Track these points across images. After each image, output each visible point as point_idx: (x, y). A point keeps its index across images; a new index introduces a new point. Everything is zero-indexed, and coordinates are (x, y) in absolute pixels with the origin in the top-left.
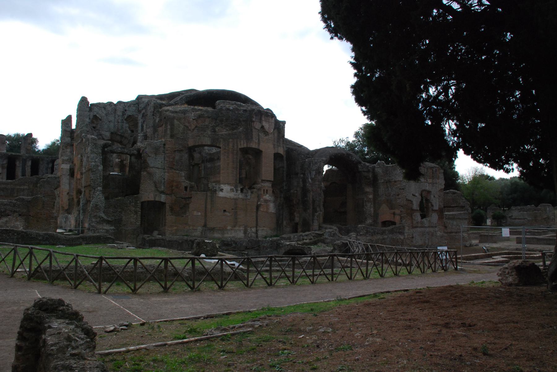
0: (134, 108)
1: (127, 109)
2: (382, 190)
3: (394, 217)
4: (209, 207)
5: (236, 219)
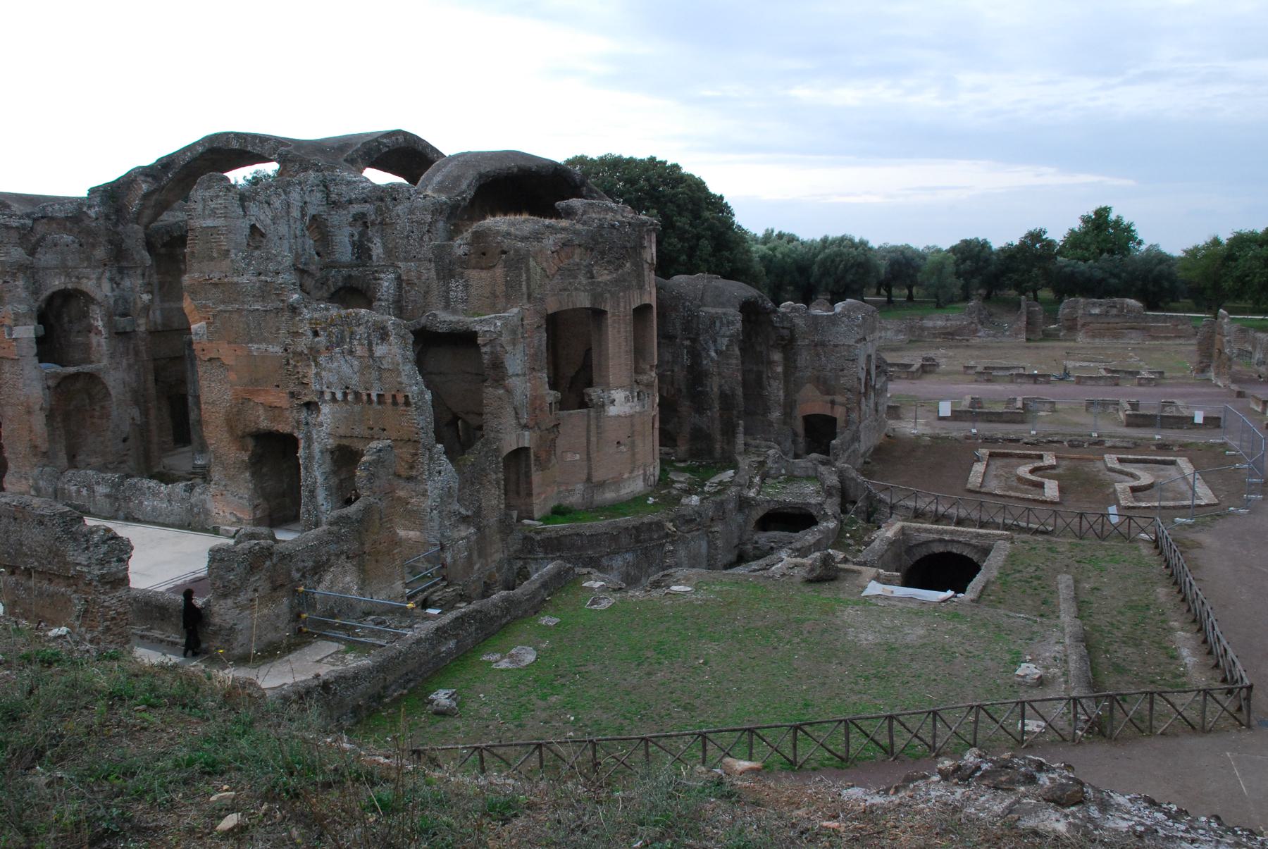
1: (308, 199)
2: (804, 358)
3: (832, 408)
4: (593, 439)
5: (634, 455)
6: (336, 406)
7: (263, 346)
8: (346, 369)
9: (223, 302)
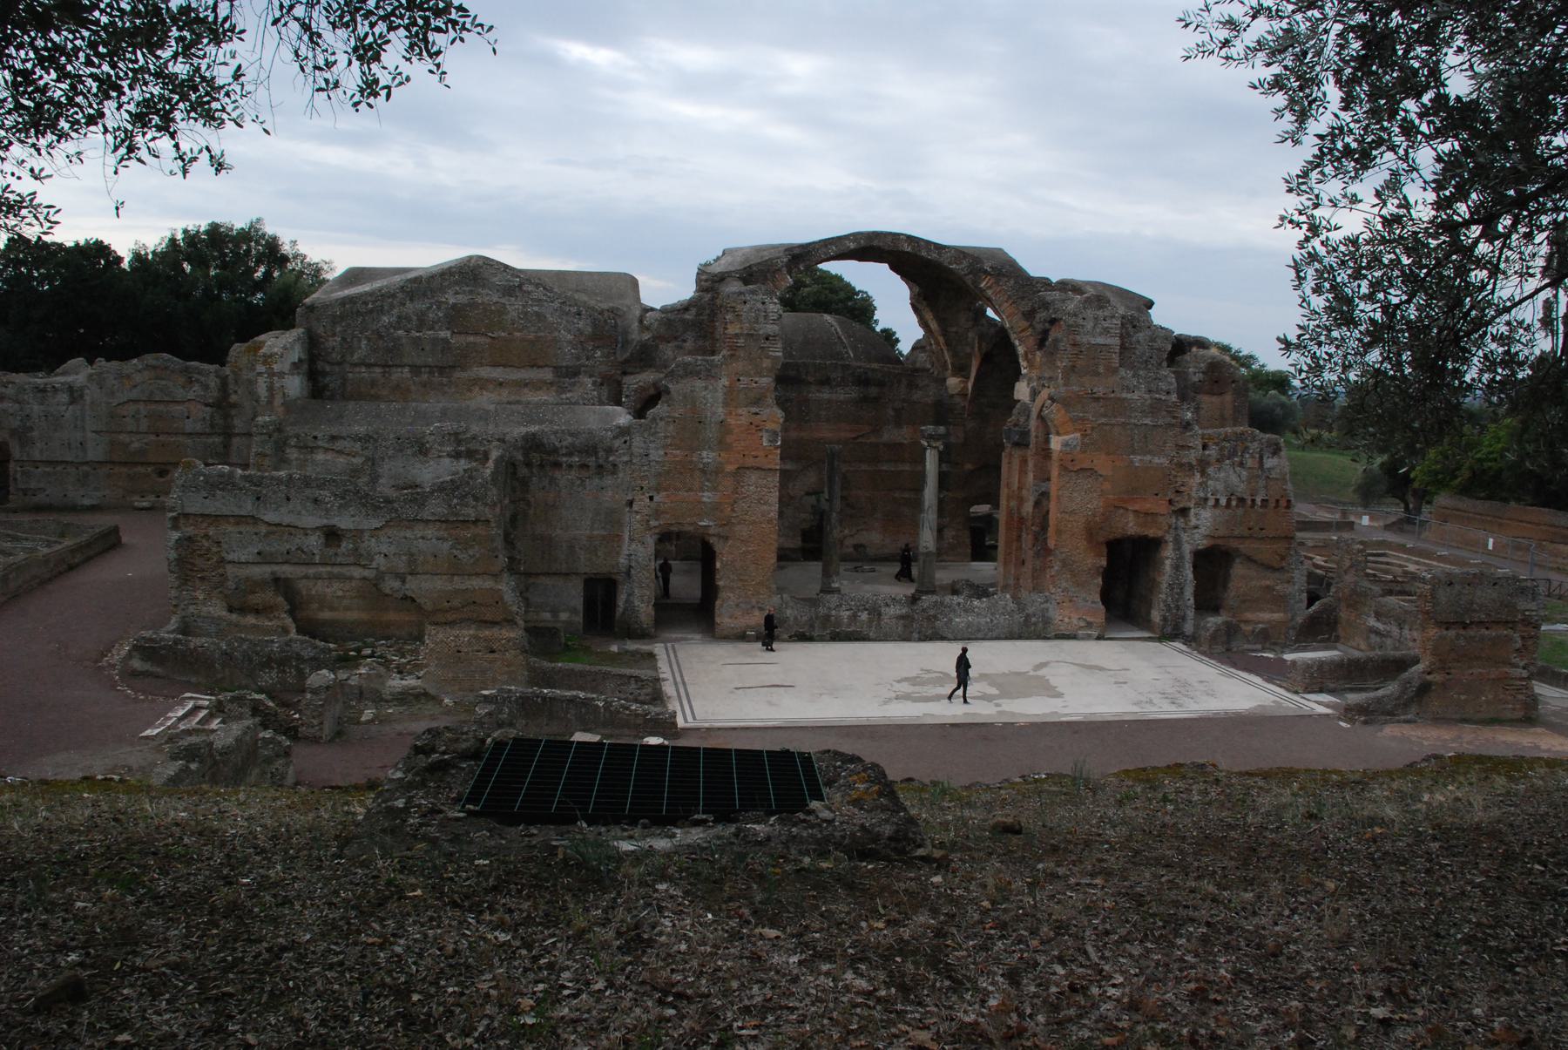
6: (1217, 512)
7: (1148, 457)
8: (1234, 479)
9: (1105, 416)
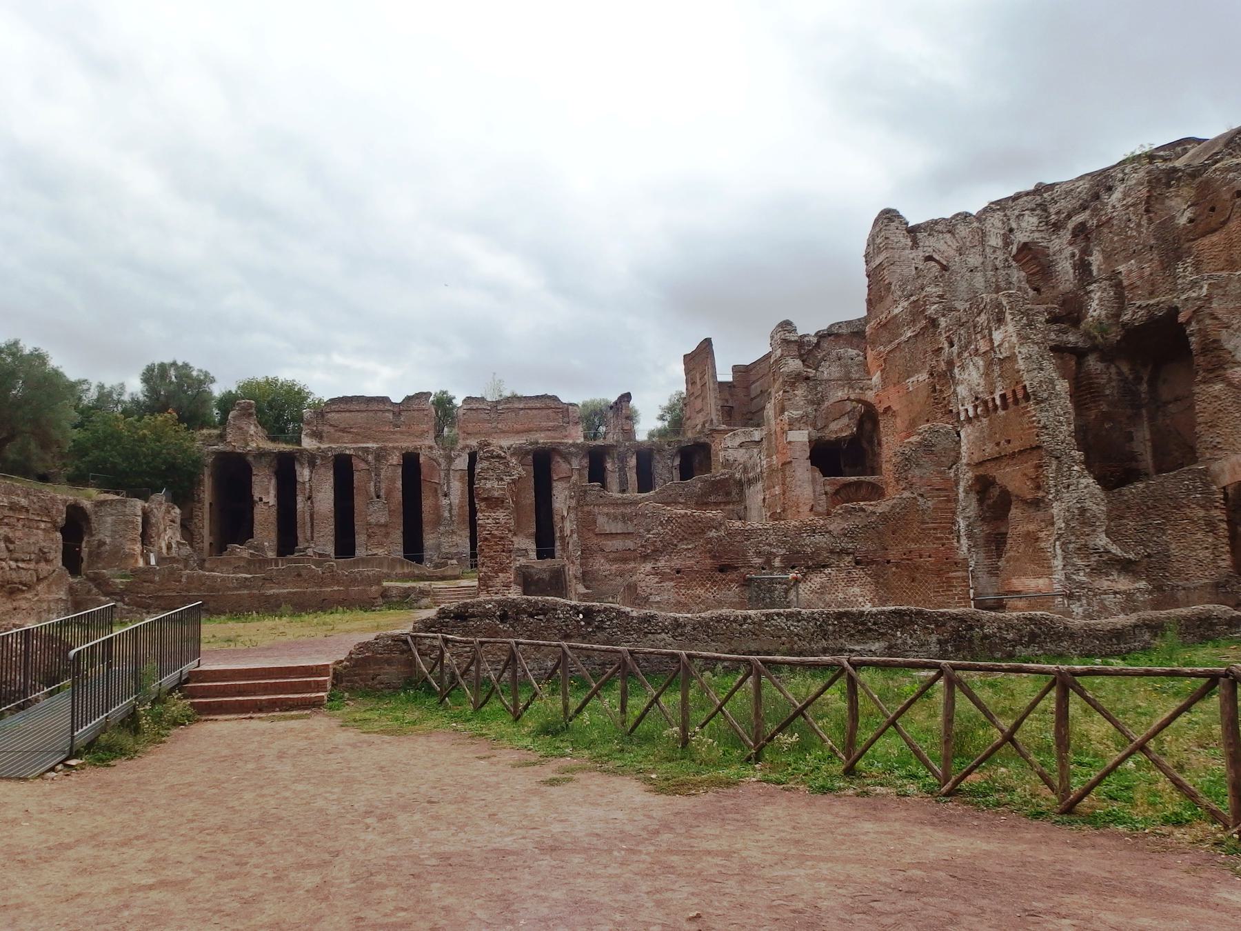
0: (1035, 220)
